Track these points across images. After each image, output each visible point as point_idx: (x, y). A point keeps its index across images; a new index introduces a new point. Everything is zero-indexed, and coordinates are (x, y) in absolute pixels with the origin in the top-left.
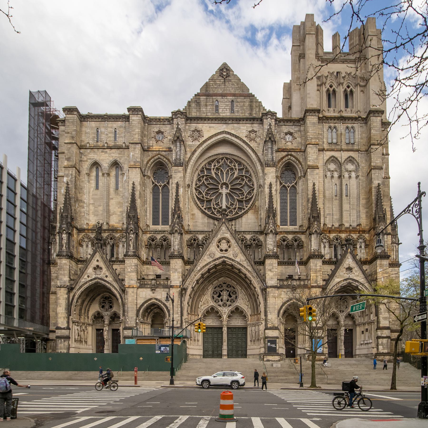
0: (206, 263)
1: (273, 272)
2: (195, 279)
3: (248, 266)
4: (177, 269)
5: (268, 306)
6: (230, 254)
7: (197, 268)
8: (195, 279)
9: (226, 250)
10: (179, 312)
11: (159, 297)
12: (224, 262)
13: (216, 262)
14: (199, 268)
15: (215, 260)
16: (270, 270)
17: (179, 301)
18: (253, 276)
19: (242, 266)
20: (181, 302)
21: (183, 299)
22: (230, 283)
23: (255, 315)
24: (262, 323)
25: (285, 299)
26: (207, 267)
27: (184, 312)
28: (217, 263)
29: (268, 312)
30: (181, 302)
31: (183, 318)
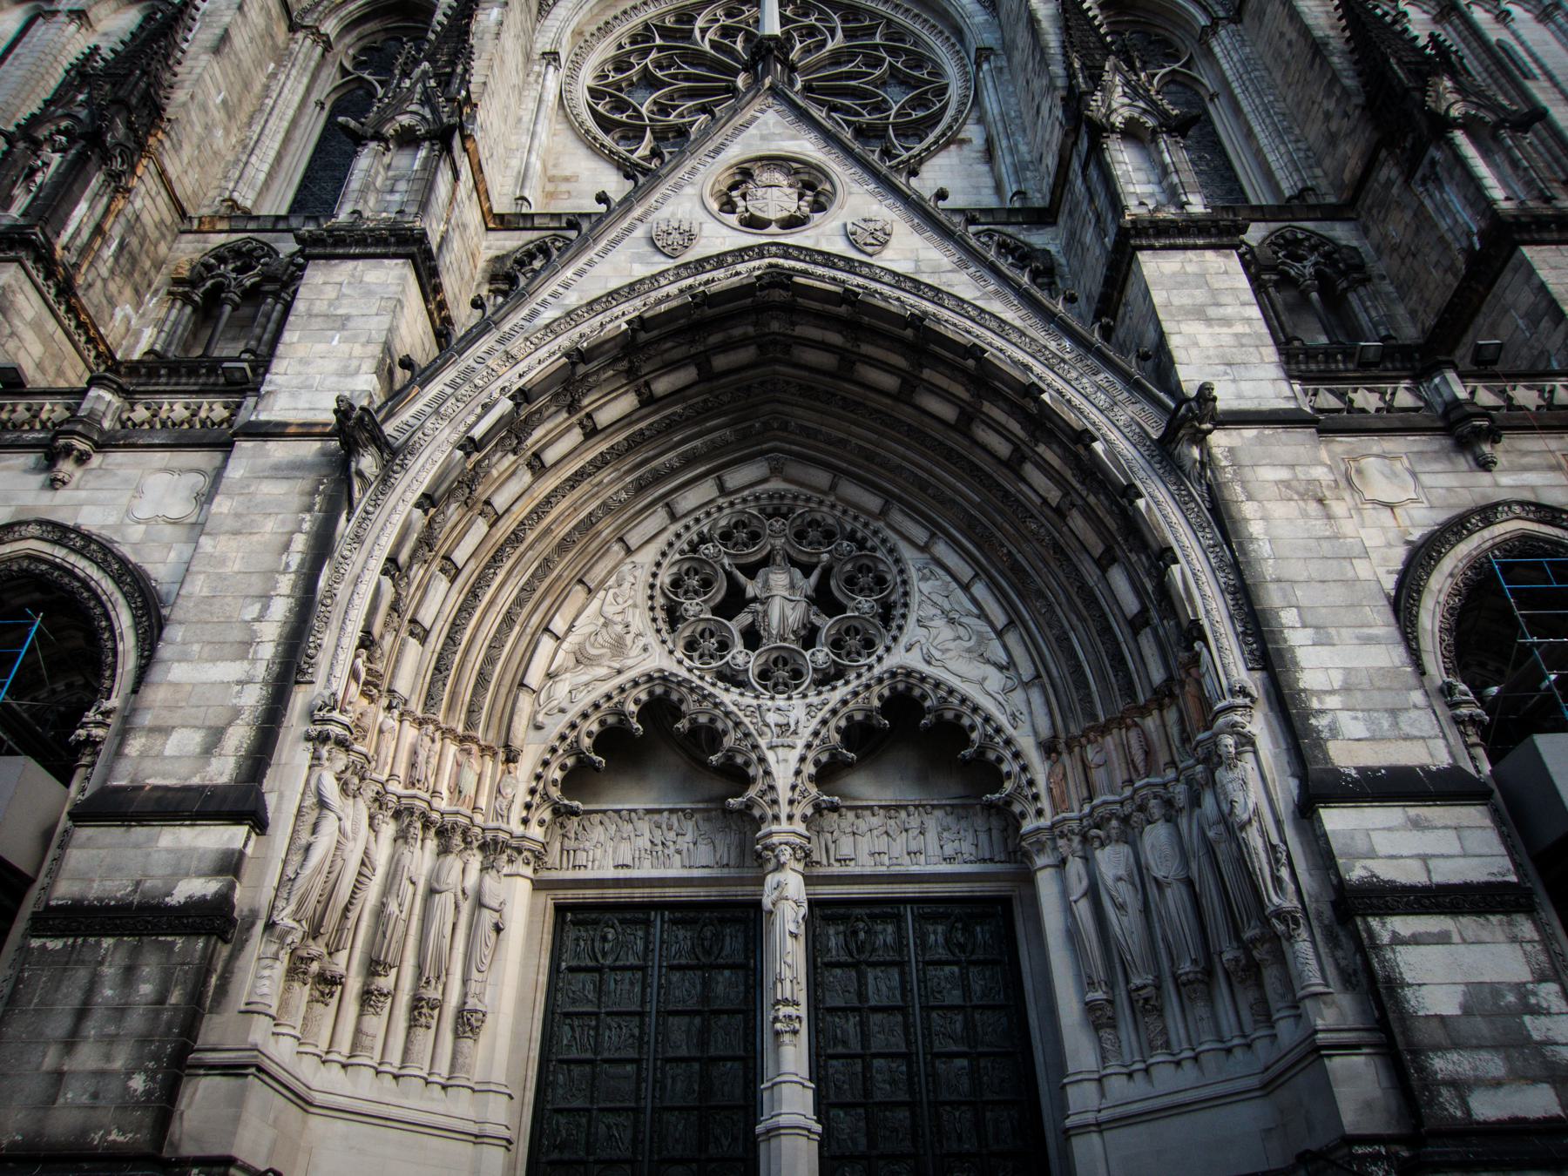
0: (614, 284)
1: (1226, 321)
2: (500, 383)
3: (989, 298)
4: (348, 317)
5: (1269, 569)
6: (825, 234)
7: (534, 314)
8: (500, 383)
9: (792, 223)
10: (270, 633)
11: (92, 519)
12: (778, 279)
13: (705, 277)
14: (548, 315)
15: (700, 265)
16: (1199, 313)
17: (300, 543)
18: (1039, 352)
19: (936, 294)
20: (322, 547)
21: (344, 527)
22: (828, 517)
23: (1104, 730)
24: (1247, 741)
25: (1421, 520)
26: (631, 308)
27: (328, 639)
28: (714, 288)
29: (1288, 617)
30: (322, 547)
31: (300, 699)
